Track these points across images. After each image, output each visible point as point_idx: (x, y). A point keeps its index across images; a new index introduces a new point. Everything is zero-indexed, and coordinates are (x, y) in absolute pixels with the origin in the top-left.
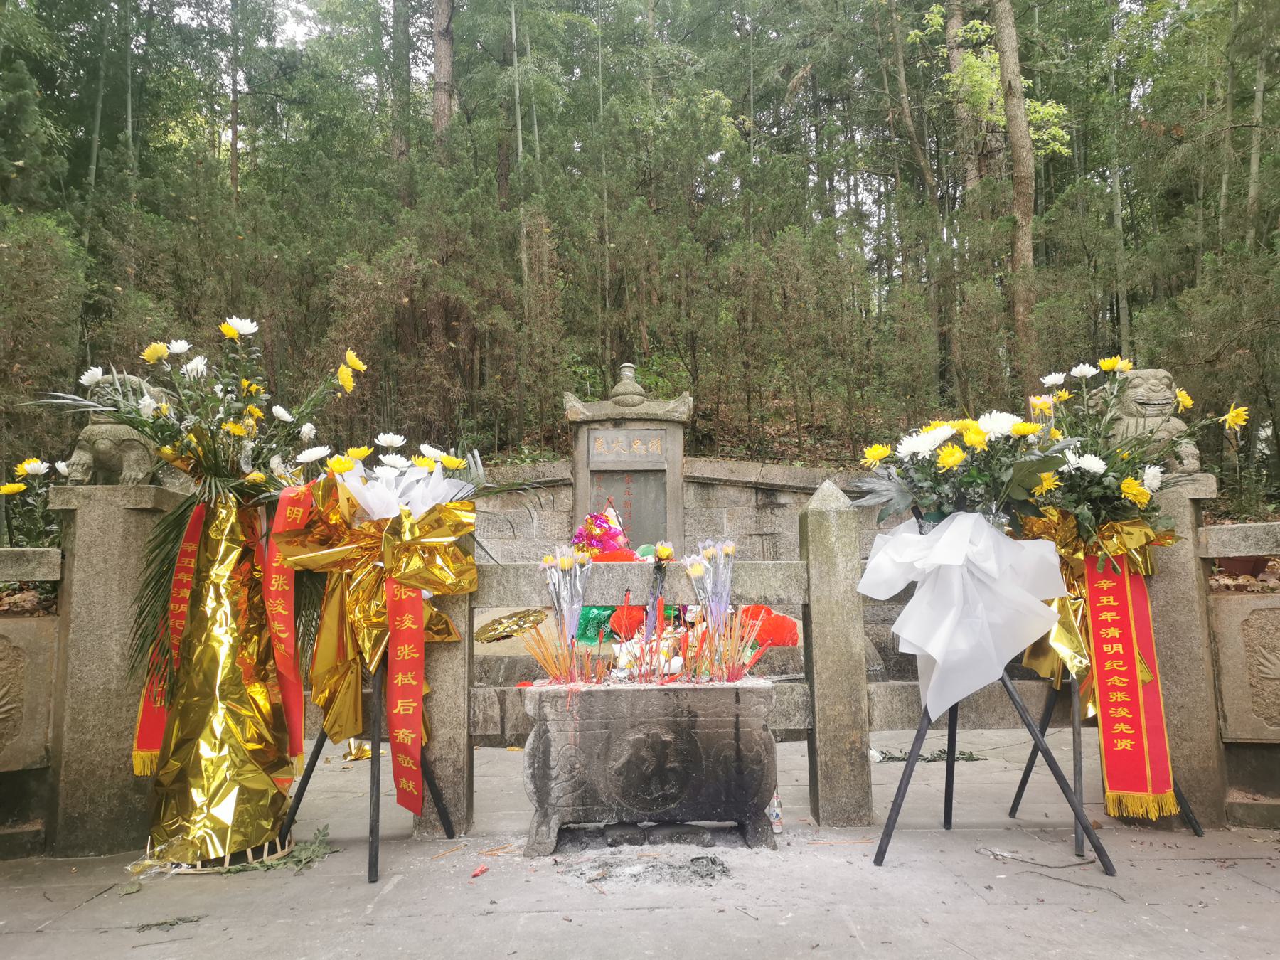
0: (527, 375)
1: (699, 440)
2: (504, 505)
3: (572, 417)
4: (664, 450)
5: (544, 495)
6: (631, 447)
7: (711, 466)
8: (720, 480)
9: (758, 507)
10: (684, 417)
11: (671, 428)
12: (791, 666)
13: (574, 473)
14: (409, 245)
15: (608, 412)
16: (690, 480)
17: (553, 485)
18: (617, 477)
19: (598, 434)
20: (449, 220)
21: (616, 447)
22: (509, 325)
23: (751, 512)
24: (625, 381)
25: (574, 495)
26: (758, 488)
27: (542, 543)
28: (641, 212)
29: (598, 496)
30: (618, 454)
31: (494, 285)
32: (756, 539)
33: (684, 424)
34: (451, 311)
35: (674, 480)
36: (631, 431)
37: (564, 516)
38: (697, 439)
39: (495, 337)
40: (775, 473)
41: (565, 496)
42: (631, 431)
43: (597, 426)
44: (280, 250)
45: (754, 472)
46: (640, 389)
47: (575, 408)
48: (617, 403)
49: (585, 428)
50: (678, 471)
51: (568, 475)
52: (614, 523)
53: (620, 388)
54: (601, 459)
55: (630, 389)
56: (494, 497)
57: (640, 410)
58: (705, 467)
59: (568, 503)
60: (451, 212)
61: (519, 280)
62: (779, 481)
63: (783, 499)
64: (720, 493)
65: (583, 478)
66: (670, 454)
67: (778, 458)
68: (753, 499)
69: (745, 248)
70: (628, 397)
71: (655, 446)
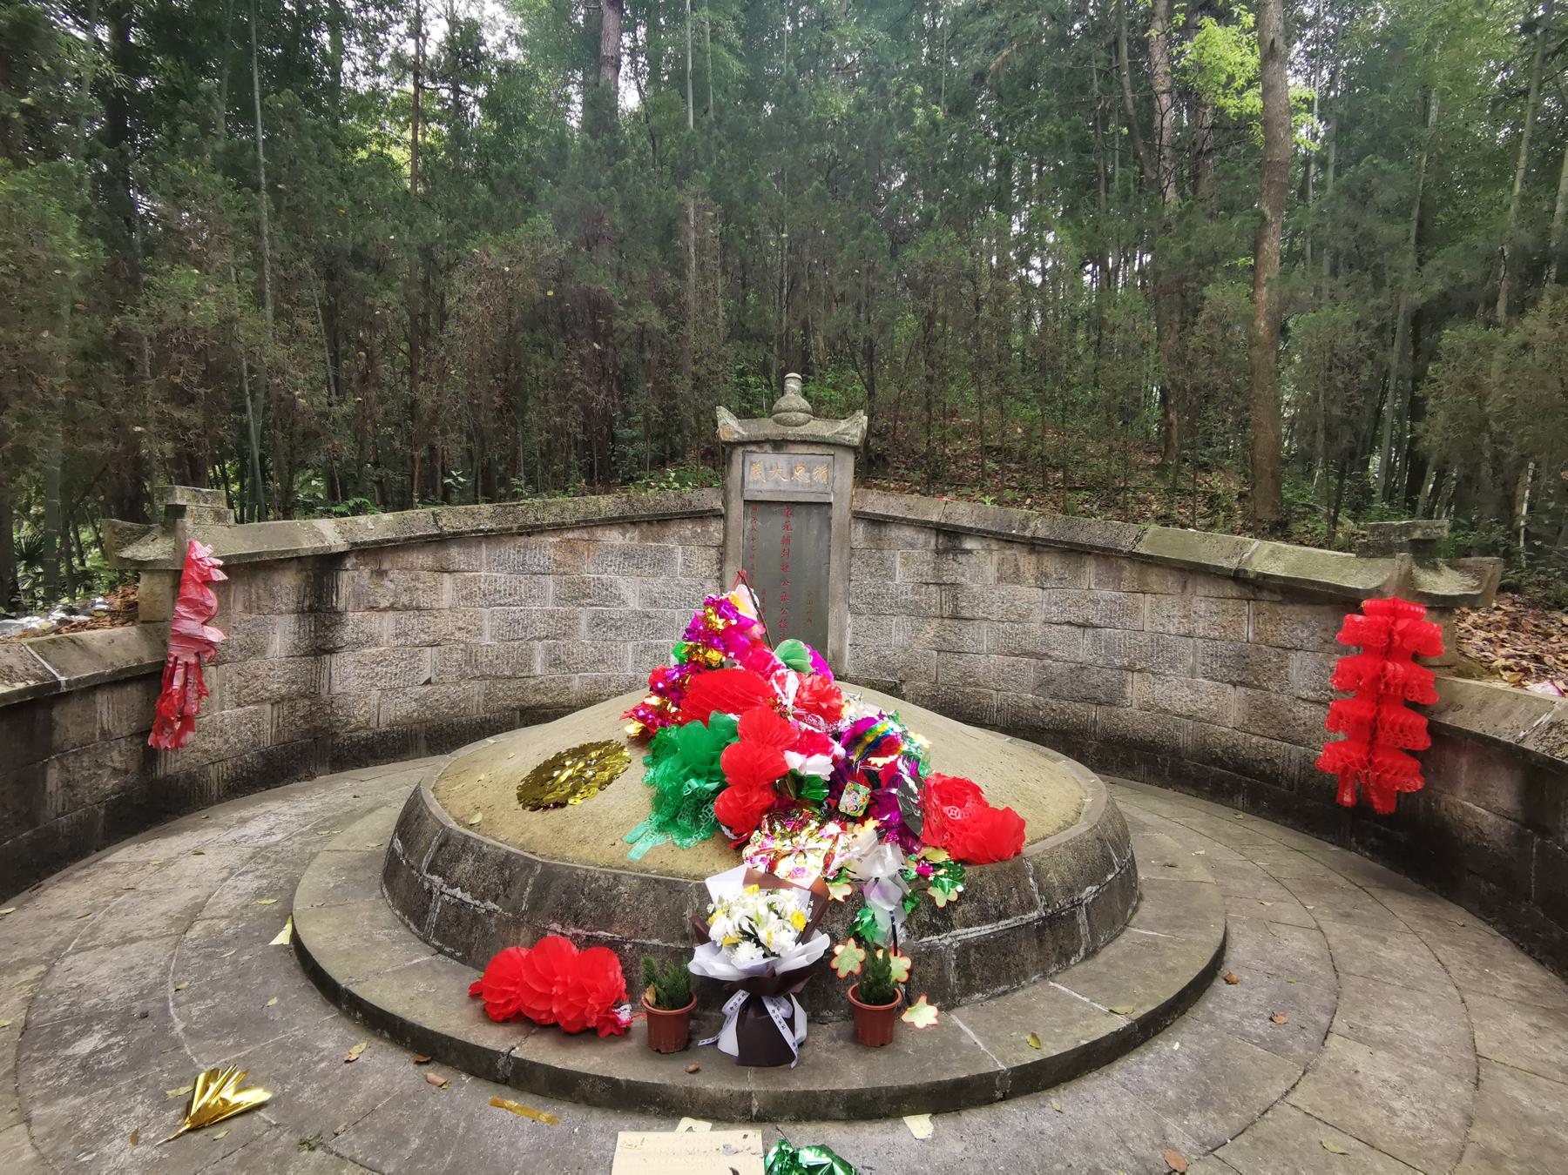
0: (683, 385)
1: (872, 464)
2: (644, 538)
3: (724, 435)
4: (831, 478)
5: (687, 529)
7: (884, 501)
8: (895, 518)
9: (937, 552)
10: (857, 441)
11: (840, 454)
12: (1014, 901)
13: (725, 503)
15: (767, 432)
16: (859, 516)
18: (775, 509)
19: (754, 457)
20: (592, 196)
21: (775, 474)
23: (929, 556)
24: (789, 394)
25: (725, 528)
26: (940, 530)
27: (686, 581)
28: (819, 195)
29: (753, 529)
30: (777, 482)
31: (645, 275)
32: (933, 588)
33: (854, 449)
34: (598, 306)
35: (840, 514)
37: (713, 552)
38: (870, 460)
39: (643, 336)
40: (961, 512)
41: (715, 527)
42: (794, 461)
43: (754, 448)
45: (936, 509)
46: (805, 403)
47: (729, 425)
48: (778, 421)
49: (740, 450)
50: (846, 504)
51: (718, 505)
52: (747, 609)
53: (782, 403)
54: (758, 487)
55: (794, 404)
56: (631, 529)
57: (804, 431)
58: (877, 503)
59: (718, 536)
60: (596, 187)
61: (680, 274)
62: (966, 522)
63: (969, 544)
64: (894, 532)
65: (736, 510)
66: (837, 486)
68: (933, 542)
69: (937, 239)
70: (791, 414)
71: (820, 474)
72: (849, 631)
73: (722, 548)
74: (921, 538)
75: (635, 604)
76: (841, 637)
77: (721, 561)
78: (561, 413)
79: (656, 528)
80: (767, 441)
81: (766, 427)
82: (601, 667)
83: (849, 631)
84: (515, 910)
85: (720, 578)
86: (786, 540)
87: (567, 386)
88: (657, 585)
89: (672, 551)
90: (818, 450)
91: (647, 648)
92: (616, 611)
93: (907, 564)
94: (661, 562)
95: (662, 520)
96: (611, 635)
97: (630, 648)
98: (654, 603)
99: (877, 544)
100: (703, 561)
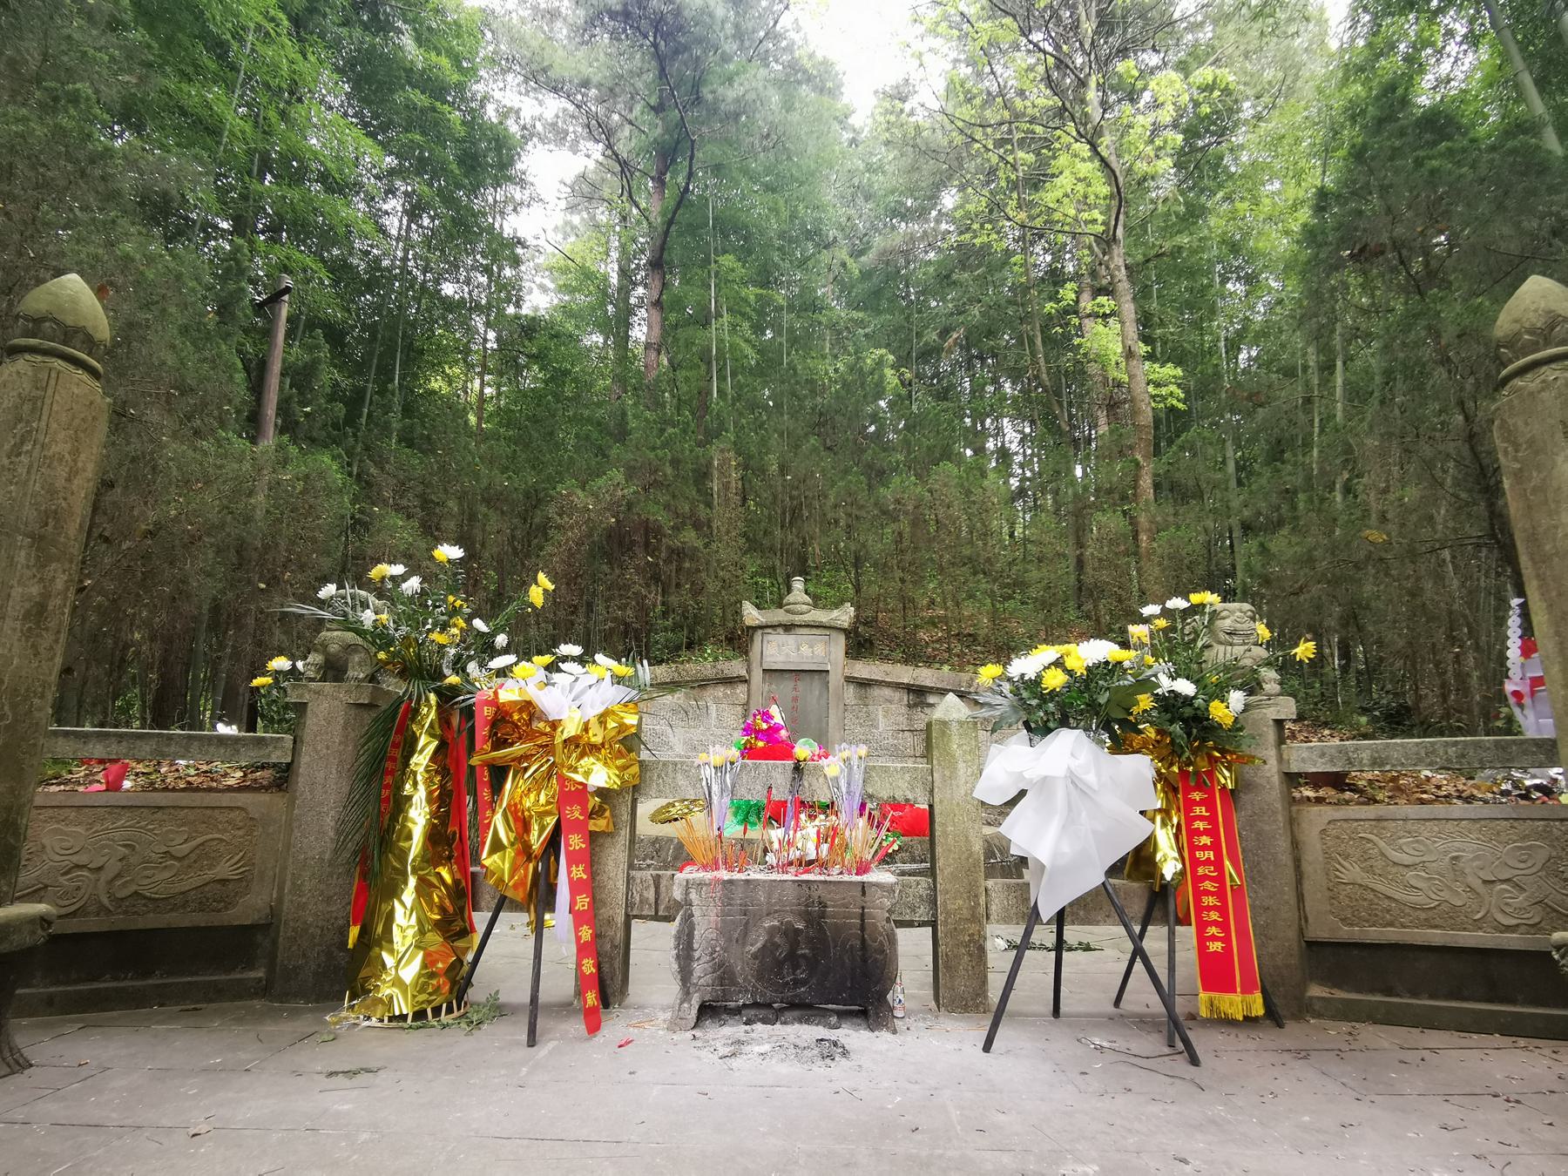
0: (712, 586)
1: (859, 644)
2: (687, 696)
4: (828, 653)
5: (720, 691)
7: (868, 668)
9: (909, 706)
10: (846, 625)
11: (834, 634)
14: (618, 475)
16: (850, 680)
17: (729, 681)
19: (770, 637)
20: (652, 456)
22: (699, 544)
23: (904, 710)
24: (795, 592)
26: (911, 689)
27: (719, 732)
28: (815, 449)
33: (844, 630)
34: (651, 531)
35: (835, 679)
36: (800, 638)
37: (739, 708)
40: (925, 676)
41: (741, 689)
42: (800, 638)
44: (509, 478)
45: (906, 674)
46: (808, 599)
47: (751, 614)
51: (743, 673)
53: (790, 598)
57: (807, 618)
58: (863, 669)
59: (743, 697)
60: (654, 449)
61: (709, 505)
62: (928, 683)
64: (876, 692)
65: (757, 676)
67: (929, 661)
71: (820, 649)
74: (897, 695)
75: (679, 749)
78: (622, 608)
80: (780, 625)
81: (779, 616)
84: (664, 861)
86: (795, 699)
87: (627, 587)
88: (696, 734)
90: (814, 631)
93: (888, 714)
95: (702, 684)
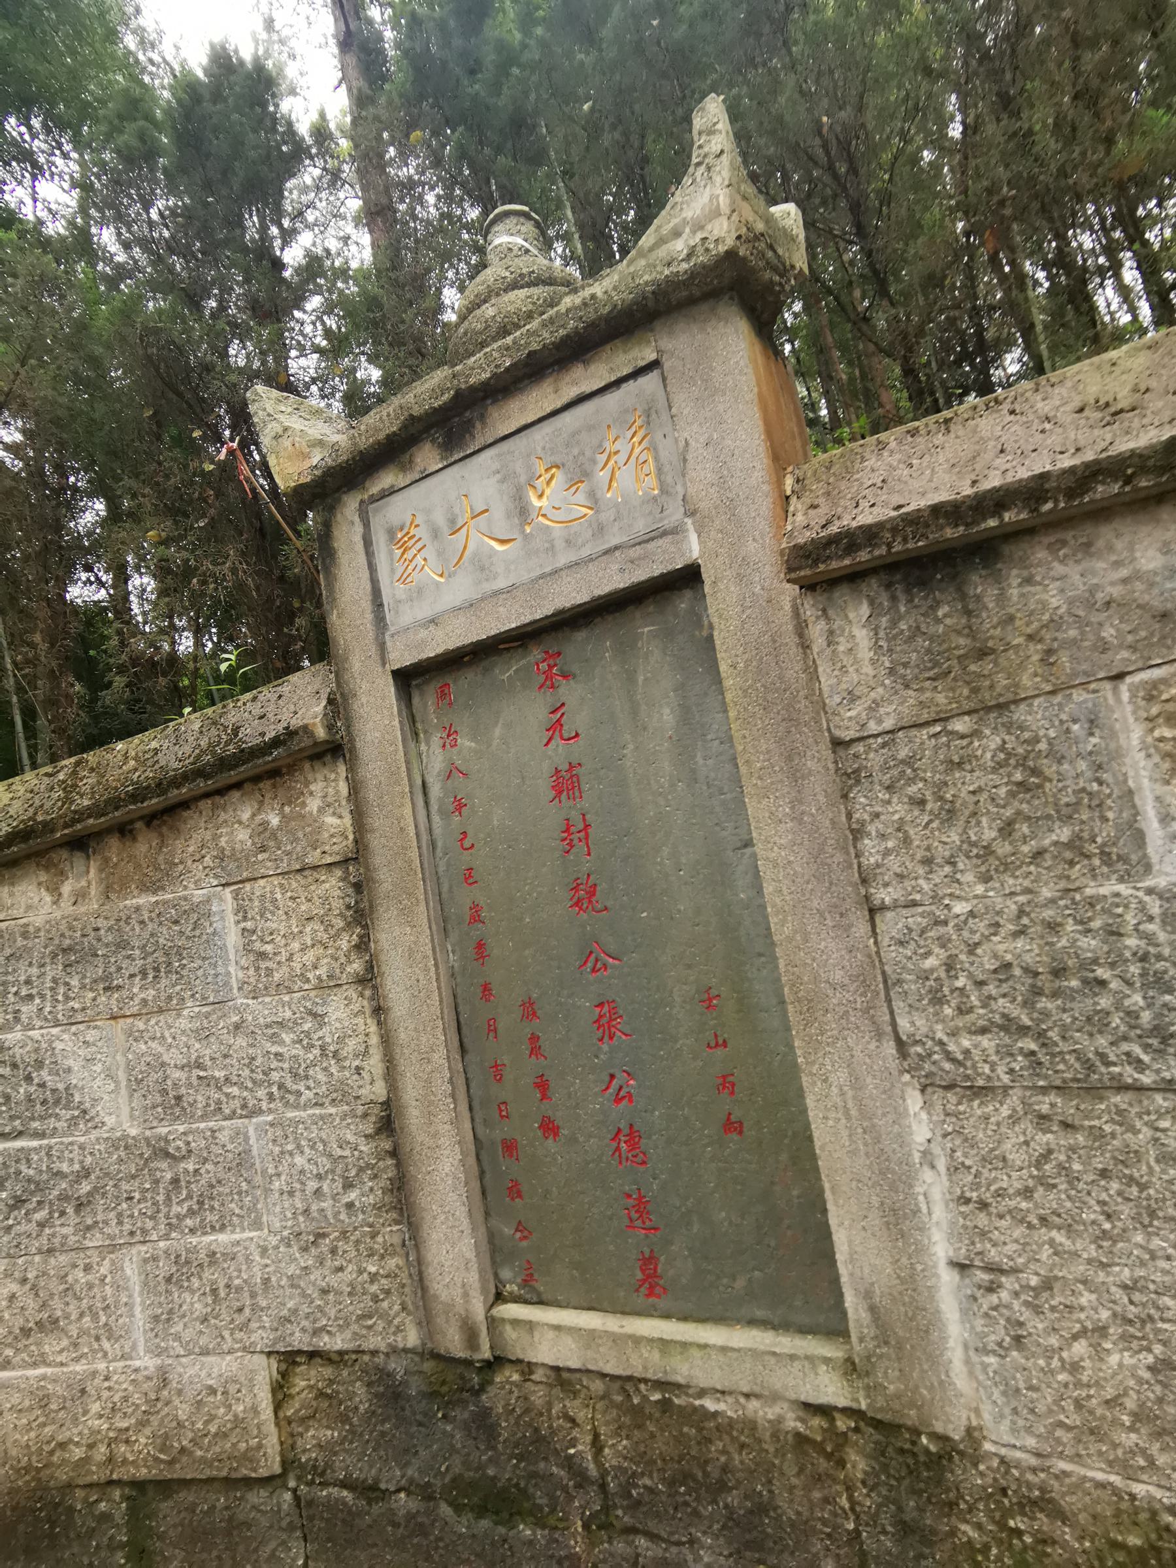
5: (240, 823)
6: (523, 512)
8: (1034, 491)
11: (676, 344)
18: (507, 670)
19: (397, 510)
27: (260, 1010)
30: (483, 566)
35: (747, 595)
41: (323, 796)
43: (387, 479)
49: (350, 505)
64: (1051, 585)
65: (377, 712)
66: (701, 479)
72: (933, 1187)
73: (355, 861)
75: (119, 1116)
76: (899, 1220)
77: (361, 916)
79: (143, 846)
82: (51, 1346)
83: (933, 1187)
85: (369, 979)
86: (566, 783)
88: (175, 1038)
89: (200, 913)
91: (184, 1268)
92: (67, 1147)
94: (172, 960)
96: (66, 1229)
97: (131, 1270)
98: (175, 1105)
99: (975, 687)
100: (301, 923)
